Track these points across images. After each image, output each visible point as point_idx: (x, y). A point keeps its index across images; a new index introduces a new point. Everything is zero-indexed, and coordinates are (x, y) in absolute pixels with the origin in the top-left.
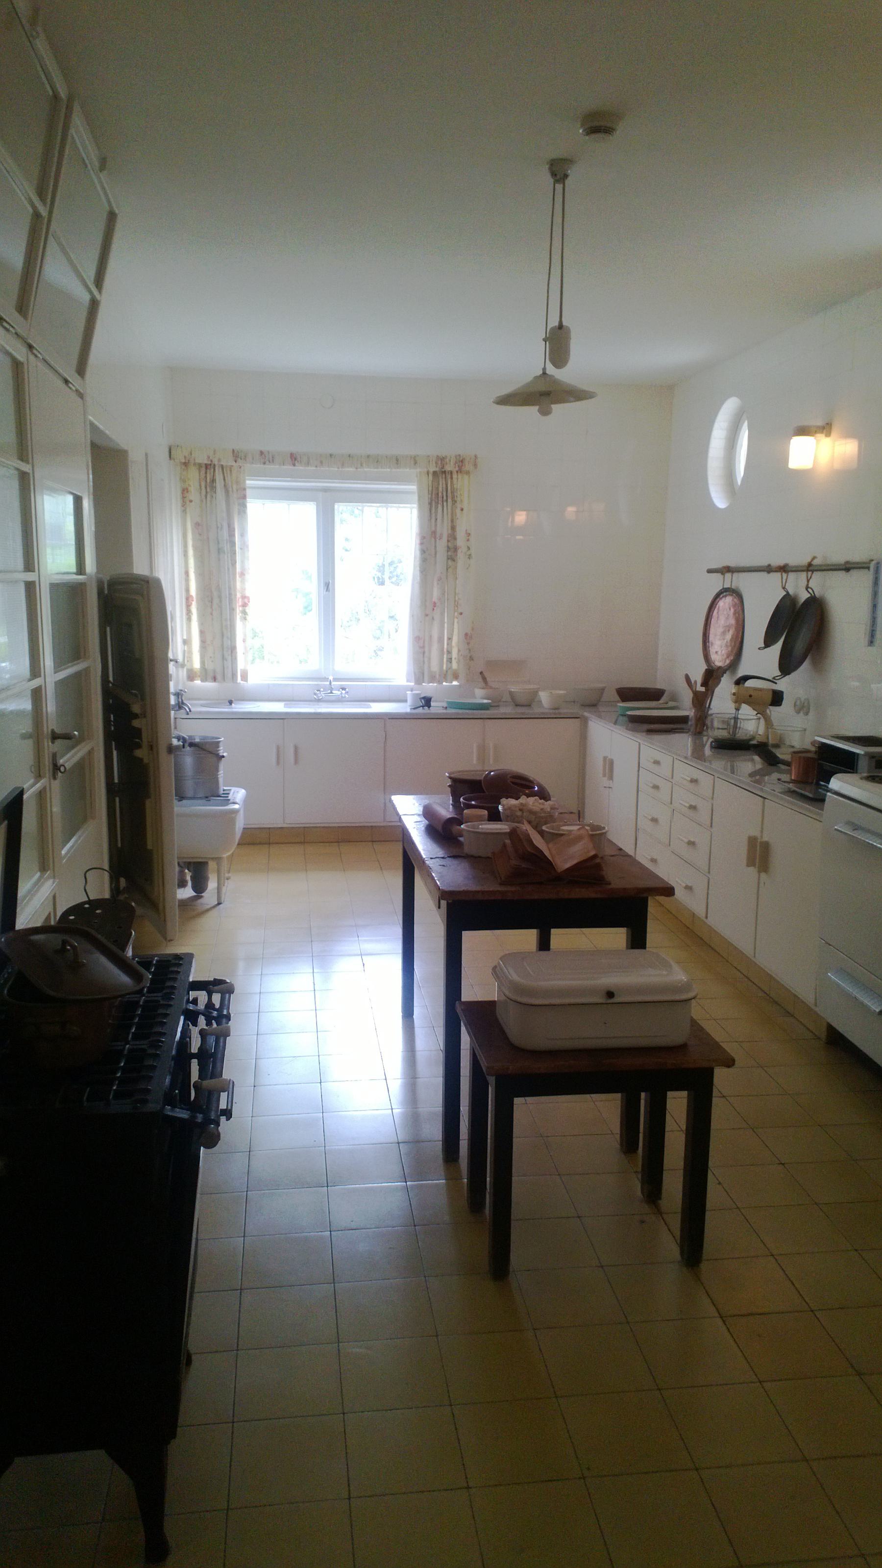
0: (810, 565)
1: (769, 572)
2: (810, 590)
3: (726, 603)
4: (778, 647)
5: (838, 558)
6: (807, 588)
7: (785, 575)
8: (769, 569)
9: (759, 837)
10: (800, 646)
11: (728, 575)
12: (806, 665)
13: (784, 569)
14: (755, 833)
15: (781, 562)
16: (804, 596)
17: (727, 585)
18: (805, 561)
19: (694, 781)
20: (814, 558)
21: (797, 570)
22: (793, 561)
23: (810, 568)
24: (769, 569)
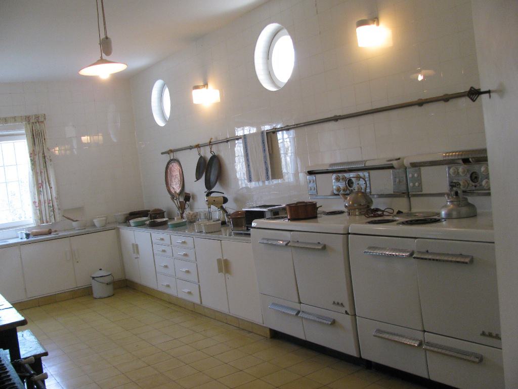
0: (210, 142)
1: (191, 149)
2: (212, 153)
3: (175, 167)
4: (203, 178)
5: (221, 138)
6: (211, 152)
7: (199, 149)
8: (191, 148)
9: (221, 258)
10: (213, 178)
11: (172, 154)
12: (218, 183)
13: (198, 146)
14: (220, 257)
15: (197, 144)
16: (209, 156)
17: (172, 158)
18: (208, 141)
19: (184, 242)
20: (211, 139)
21: (204, 145)
22: (201, 142)
23: (210, 144)
24: (191, 148)
